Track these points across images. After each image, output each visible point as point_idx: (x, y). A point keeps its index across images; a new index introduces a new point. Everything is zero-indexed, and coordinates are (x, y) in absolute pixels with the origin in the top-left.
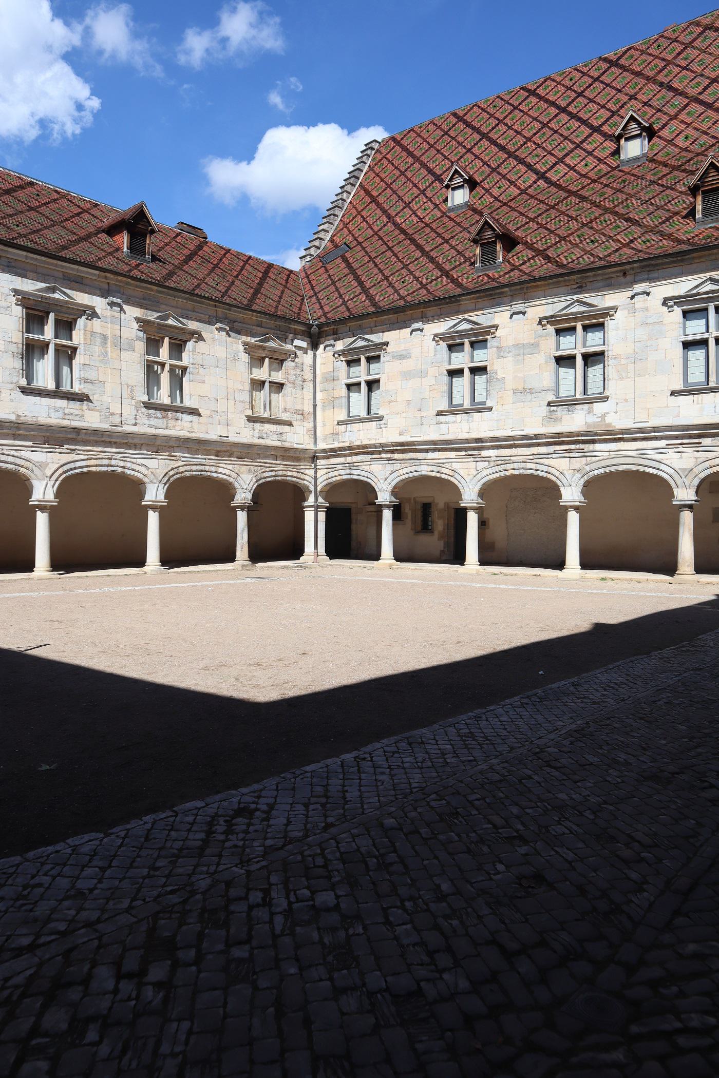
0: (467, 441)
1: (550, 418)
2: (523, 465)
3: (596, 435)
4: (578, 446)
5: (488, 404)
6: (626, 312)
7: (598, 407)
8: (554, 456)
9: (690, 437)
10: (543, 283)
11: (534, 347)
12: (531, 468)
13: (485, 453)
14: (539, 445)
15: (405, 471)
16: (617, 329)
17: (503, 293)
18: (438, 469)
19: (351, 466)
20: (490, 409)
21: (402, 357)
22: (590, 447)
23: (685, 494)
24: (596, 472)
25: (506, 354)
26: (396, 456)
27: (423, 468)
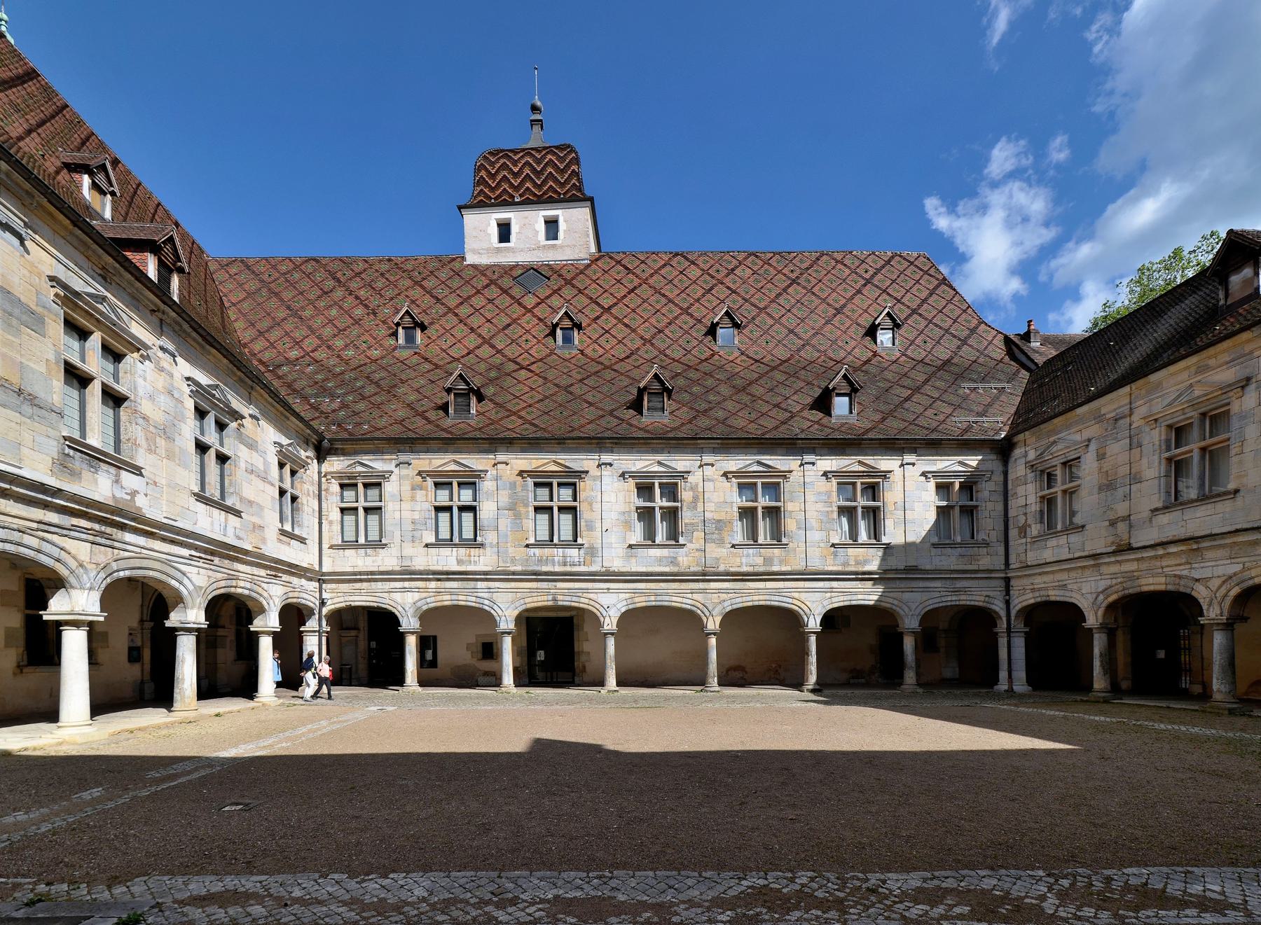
4: (109, 530)
8: (73, 534)
9: (206, 551)
22: (117, 534)
23: (713, 624)
24: (122, 574)
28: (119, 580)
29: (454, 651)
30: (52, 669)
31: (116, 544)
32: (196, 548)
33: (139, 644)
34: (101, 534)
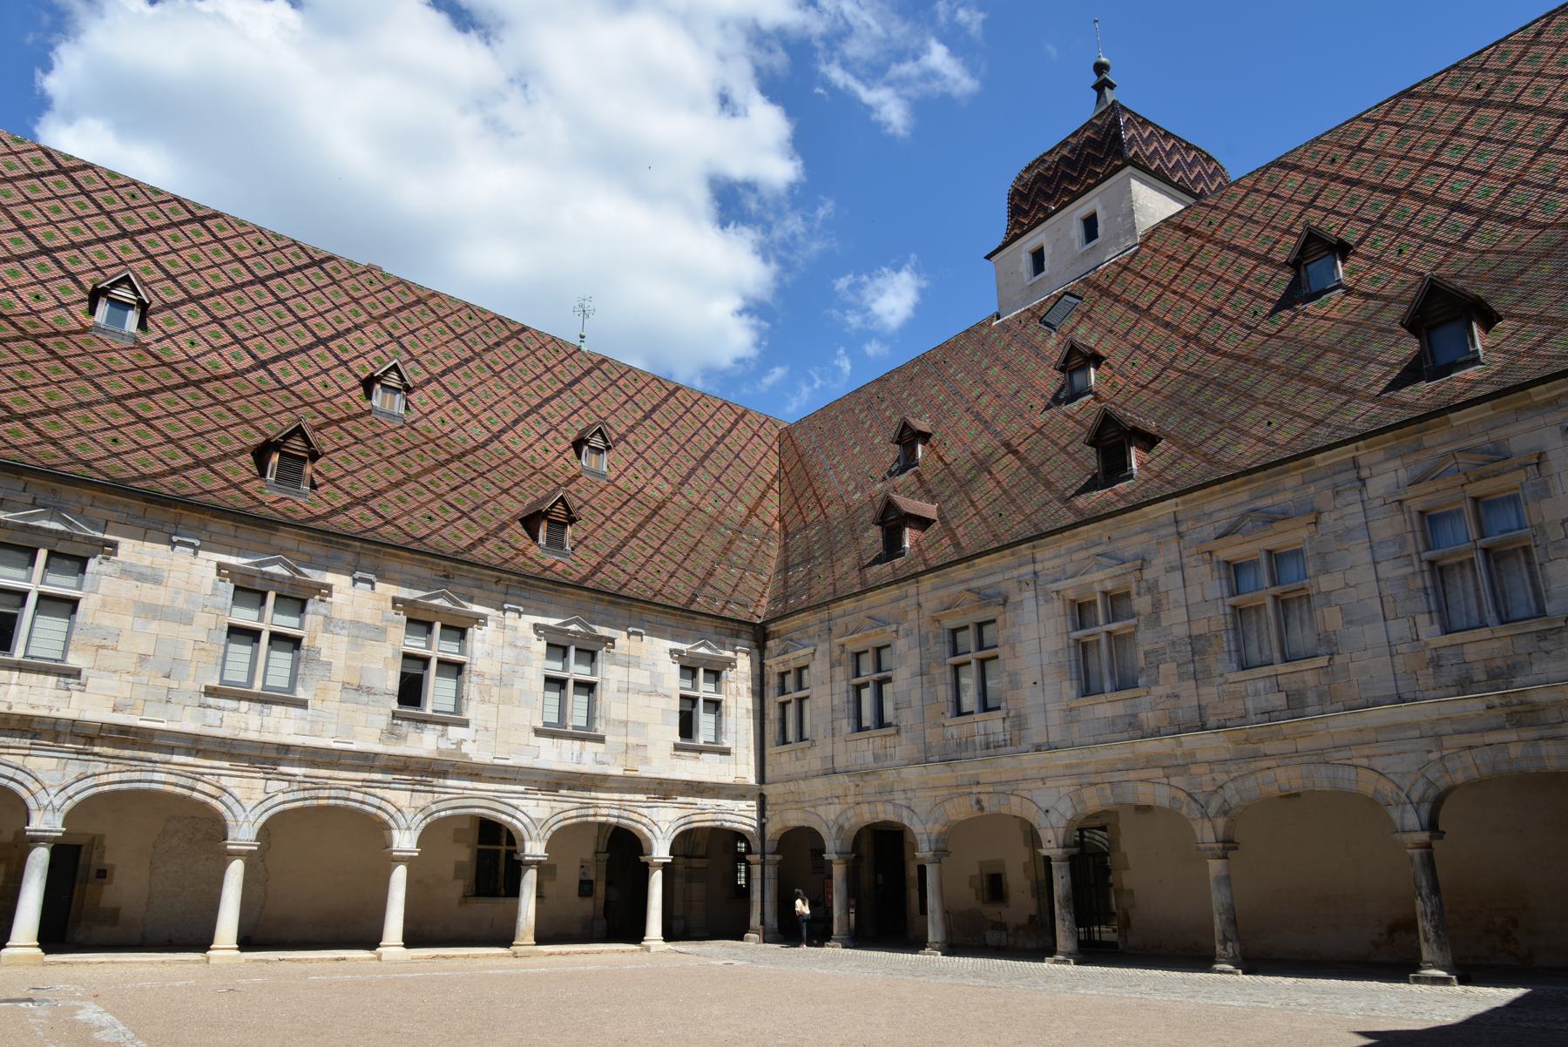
1: (391, 734)
2: (344, 794)
7: (455, 732)
11: (379, 633)
15: (116, 777)
18: (190, 782)
20: (303, 704)
21: (141, 577)
25: (337, 630)
27: (156, 776)
29: (128, 885)
30: (509, 900)
33: (592, 877)
34: (420, 783)
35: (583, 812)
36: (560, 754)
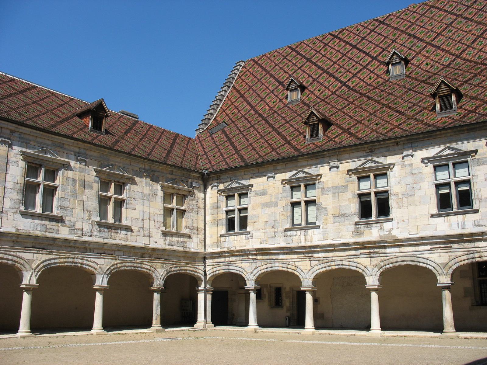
0: (305, 247)
1: (357, 233)
2: (341, 263)
3: (386, 242)
5: (317, 224)
6: (400, 166)
8: (360, 256)
9: (444, 243)
10: (348, 149)
11: (345, 188)
12: (346, 264)
13: (316, 255)
14: (350, 250)
15: (265, 267)
16: (395, 177)
17: (324, 155)
18: (286, 266)
19: (229, 264)
20: (319, 227)
21: (261, 194)
22: (383, 250)
23: (444, 279)
24: (388, 266)
25: (327, 193)
26: (259, 257)
27: (276, 265)
28: (386, 269)
31: (381, 255)
32: (436, 243)
35: (471, 256)
36: (450, 225)
